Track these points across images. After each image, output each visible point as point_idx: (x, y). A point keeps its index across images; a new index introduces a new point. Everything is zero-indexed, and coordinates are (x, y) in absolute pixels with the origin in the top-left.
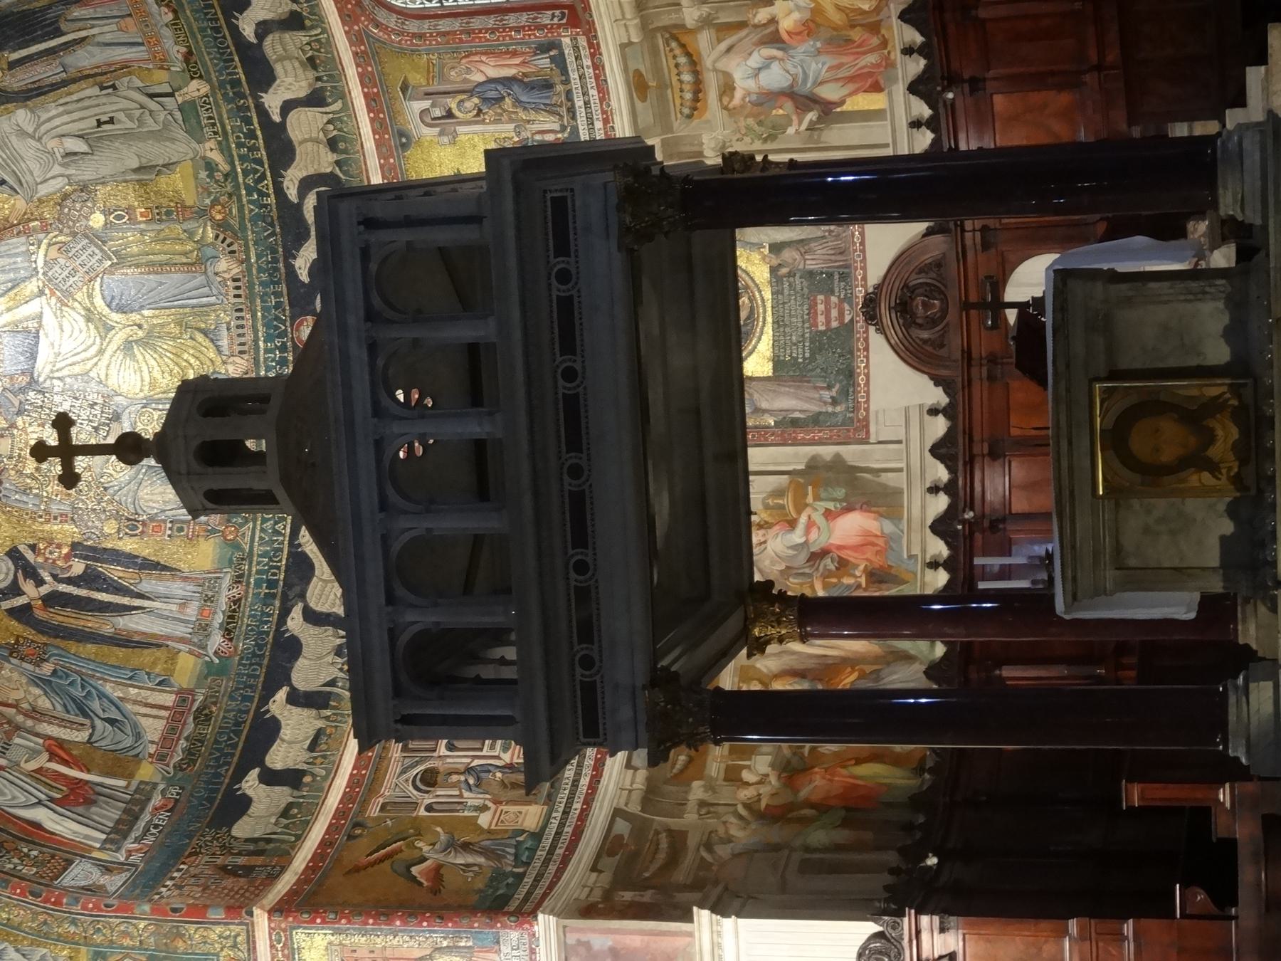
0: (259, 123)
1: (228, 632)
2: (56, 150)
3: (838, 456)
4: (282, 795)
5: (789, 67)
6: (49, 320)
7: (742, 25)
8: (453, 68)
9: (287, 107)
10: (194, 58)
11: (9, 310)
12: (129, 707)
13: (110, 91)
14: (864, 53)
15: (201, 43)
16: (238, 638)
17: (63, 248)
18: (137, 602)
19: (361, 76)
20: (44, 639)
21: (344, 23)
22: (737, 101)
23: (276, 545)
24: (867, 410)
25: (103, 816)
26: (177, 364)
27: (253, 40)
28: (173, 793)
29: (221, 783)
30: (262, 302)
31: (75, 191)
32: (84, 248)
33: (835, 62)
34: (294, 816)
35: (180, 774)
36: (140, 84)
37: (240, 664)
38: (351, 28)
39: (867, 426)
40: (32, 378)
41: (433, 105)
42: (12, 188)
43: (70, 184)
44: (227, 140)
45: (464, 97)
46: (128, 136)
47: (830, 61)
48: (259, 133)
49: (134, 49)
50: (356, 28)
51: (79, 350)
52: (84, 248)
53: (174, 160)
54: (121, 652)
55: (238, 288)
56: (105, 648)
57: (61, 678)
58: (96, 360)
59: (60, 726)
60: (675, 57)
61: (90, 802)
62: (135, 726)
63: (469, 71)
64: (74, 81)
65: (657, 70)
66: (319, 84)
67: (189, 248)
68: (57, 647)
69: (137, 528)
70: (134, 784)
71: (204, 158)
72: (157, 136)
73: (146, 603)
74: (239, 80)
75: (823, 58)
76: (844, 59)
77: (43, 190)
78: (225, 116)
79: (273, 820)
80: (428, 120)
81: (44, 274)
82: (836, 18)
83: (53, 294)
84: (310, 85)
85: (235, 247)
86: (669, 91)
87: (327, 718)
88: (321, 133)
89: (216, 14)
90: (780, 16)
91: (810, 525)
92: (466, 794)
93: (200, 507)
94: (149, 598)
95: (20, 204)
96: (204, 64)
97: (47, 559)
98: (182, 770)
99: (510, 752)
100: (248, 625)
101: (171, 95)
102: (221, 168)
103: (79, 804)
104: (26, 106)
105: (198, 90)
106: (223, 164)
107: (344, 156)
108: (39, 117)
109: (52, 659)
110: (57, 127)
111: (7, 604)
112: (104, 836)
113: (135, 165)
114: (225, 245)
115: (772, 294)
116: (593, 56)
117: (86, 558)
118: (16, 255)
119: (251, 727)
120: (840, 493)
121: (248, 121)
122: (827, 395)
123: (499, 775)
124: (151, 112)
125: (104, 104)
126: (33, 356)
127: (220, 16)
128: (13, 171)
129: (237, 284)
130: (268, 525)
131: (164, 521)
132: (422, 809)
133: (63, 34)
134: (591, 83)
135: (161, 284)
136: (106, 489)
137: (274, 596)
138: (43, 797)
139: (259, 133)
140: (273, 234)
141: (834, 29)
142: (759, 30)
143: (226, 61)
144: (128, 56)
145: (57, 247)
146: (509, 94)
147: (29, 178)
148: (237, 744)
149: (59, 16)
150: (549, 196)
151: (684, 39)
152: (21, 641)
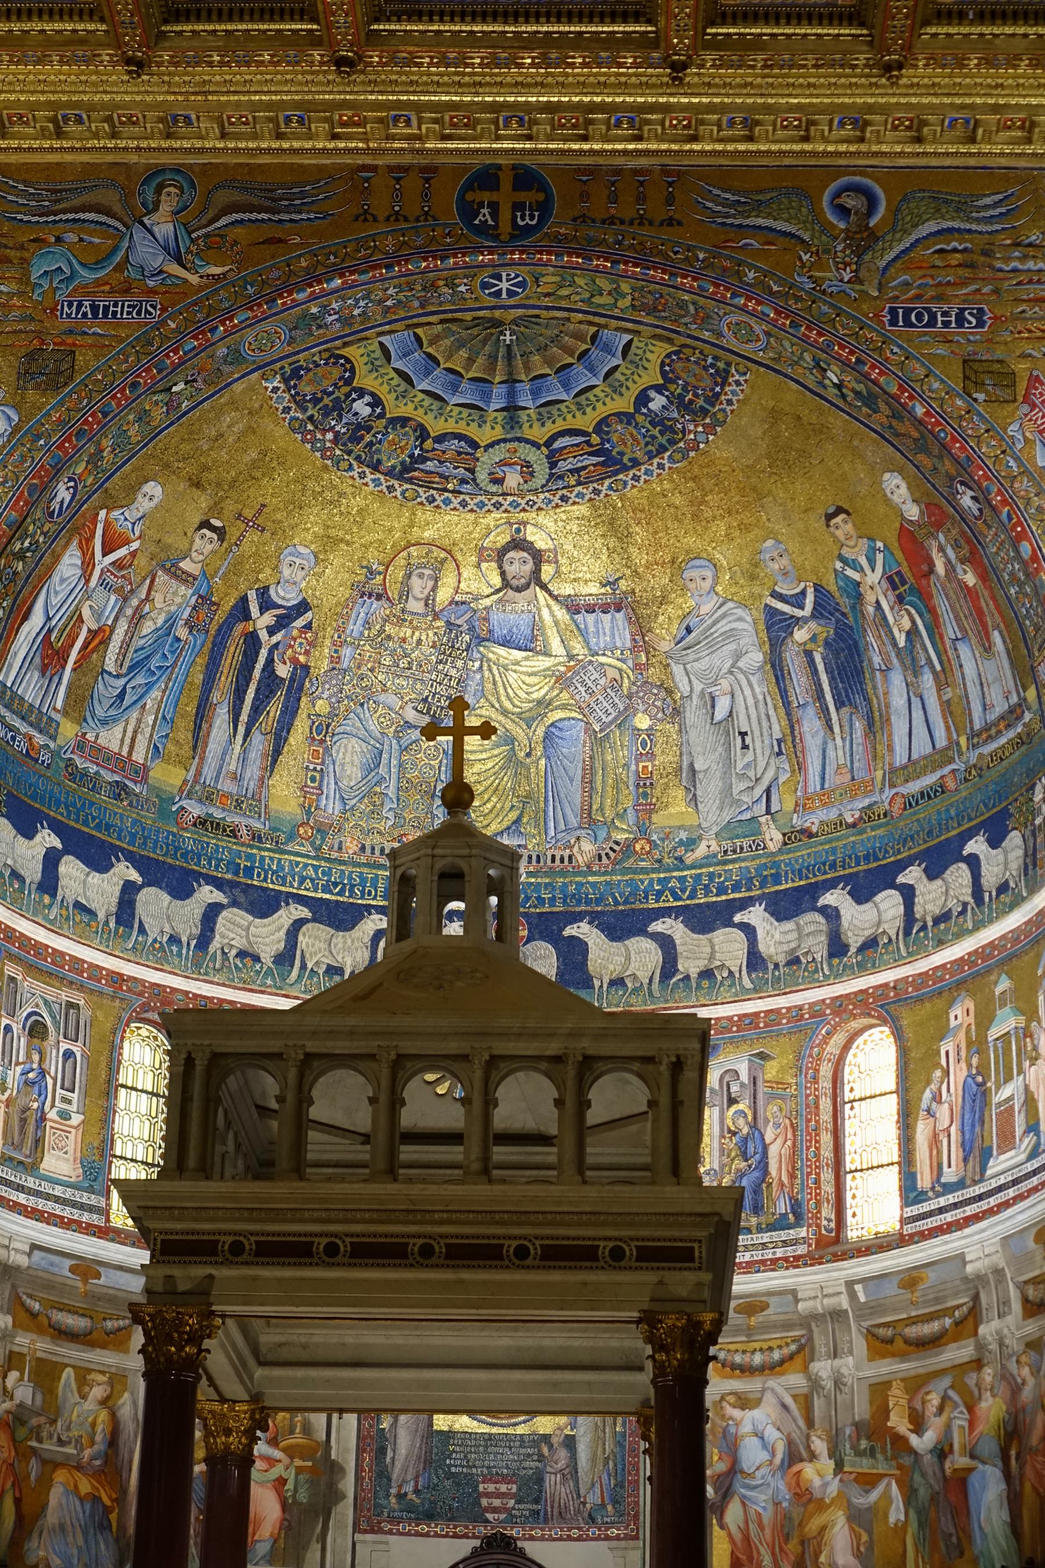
0: (734, 900)
1: (202, 822)
3: (343, 1497)
4: (33, 872)
5: (763, 1471)
6: (543, 663)
7: (810, 1423)
8: (781, 1110)
9: (749, 930)
11: (556, 623)
12: (135, 715)
13: (776, 749)
14: (773, 1554)
15: (820, 848)
16: (195, 833)
17: (615, 684)
18: (241, 729)
19: (777, 1011)
20: (213, 632)
21: (834, 999)
22: (730, 1411)
23: (289, 878)
24: (390, 1532)
25: (29, 683)
26: (487, 789)
27: (821, 902)
28: (45, 757)
29: (49, 808)
30: (546, 884)
31: (675, 702)
32: (614, 705)
33: (765, 1521)
34: (11, 885)
35: (62, 765)
36: (781, 781)
37: (169, 832)
38: (828, 1006)
39: (372, 1531)
40: (485, 640)
41: (742, 1085)
42: (682, 639)
43: (682, 698)
45: (750, 1118)
46: (729, 762)
47: (767, 1517)
48: (724, 898)
49: (818, 779)
50: (828, 1012)
51: (509, 690)
52: (614, 705)
53: (700, 807)
54: (191, 709)
55: (562, 860)
56: (198, 693)
57: (171, 645)
58: (497, 705)
59: (122, 642)
60: (780, 1347)
61: (43, 673)
62: (115, 720)
63: (777, 1126)
64: (788, 714)
65: (767, 1327)
66: (771, 966)
67: (609, 813)
68: (203, 645)
69: (318, 734)
70: (57, 716)
71: (700, 838)
72: (727, 790)
73: (239, 738)
74: (780, 884)
75: (770, 1508)
76: (768, 1532)
77: (677, 670)
78: (743, 865)
79: (9, 862)
80: (727, 1078)
81: (591, 662)
82: (813, 1525)
83: (569, 668)
84: (770, 957)
85: (605, 860)
86: (744, 1339)
87: (107, 922)
88: (719, 963)
89: (850, 867)
90: (818, 1465)
91: (271, 1462)
92: (19, 1069)
93: (398, 862)
94: (245, 740)
95: (665, 646)
97: (295, 639)
98: (67, 766)
99: (58, 1119)
100: (208, 844)
101: (768, 812)
103: (43, 659)
107: (694, 985)
109: (191, 638)
111: (252, 595)
112: (9, 684)
113: (697, 767)
114: (608, 850)
115: (521, 1435)
116: (786, 1259)
117: (292, 680)
118: (613, 636)
119: (104, 841)
120: (303, 1497)
121: (736, 888)
122: (409, 1488)
123: (35, 1105)
124: (752, 788)
126: (506, 643)
127: (847, 872)
129: (566, 860)
130: (311, 872)
131: (323, 763)
132: (8, 1022)
133: (837, 710)
134: (758, 1255)
135: (572, 781)
136: (362, 705)
137: (237, 874)
138: (54, 622)
139: (724, 898)
140: (617, 903)
141: (800, 1524)
142: (804, 1440)
144: (811, 771)
145: (618, 677)
146: (750, 1166)
147: (691, 657)
148: (88, 826)
149: (856, 708)
150: (696, 1245)
151: (798, 1360)
152: (214, 608)
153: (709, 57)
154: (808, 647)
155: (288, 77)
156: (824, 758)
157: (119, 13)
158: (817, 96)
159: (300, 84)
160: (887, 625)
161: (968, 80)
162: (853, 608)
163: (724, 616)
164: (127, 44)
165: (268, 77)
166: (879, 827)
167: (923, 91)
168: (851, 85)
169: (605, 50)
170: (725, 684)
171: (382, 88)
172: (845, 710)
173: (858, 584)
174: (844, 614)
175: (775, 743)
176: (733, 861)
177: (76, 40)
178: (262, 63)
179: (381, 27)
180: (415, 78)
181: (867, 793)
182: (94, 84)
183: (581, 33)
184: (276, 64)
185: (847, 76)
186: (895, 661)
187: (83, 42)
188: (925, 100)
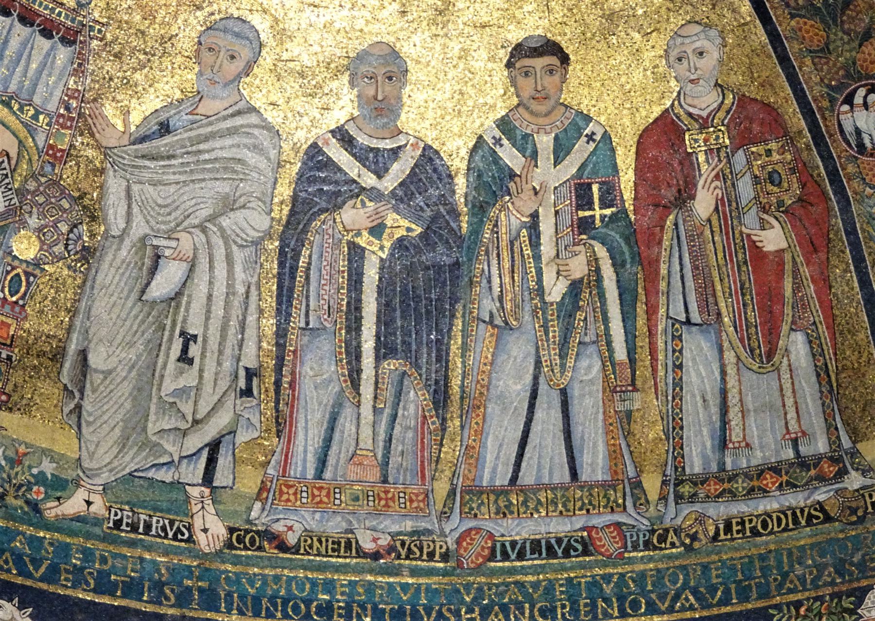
2: (173, 244)
10: (270, 550)
13: (242, 383)
44: (105, 538)
48: (106, 600)
49: (311, 460)
71: (78, 486)
77: (115, 185)
96: (248, 562)
102: (49, 505)
104: (268, 235)
105: (205, 530)
106: (59, 511)
108: (242, 246)
110: (211, 268)
113: (94, 360)
124: (185, 433)
125: (219, 364)
128: (173, 157)
139: (106, 600)
143: (257, 600)
145: (13, 154)
147: (146, 175)
149: (418, 367)
154: (362, 242)
156: (331, 429)
160: (537, 257)
162: (480, 209)
163: (232, 132)
166: (430, 572)
170: (186, 242)
172: (391, 365)
173: (512, 175)
174: (455, 213)
175: (242, 373)
176: (132, 544)
181: (419, 513)
186: (527, 317)
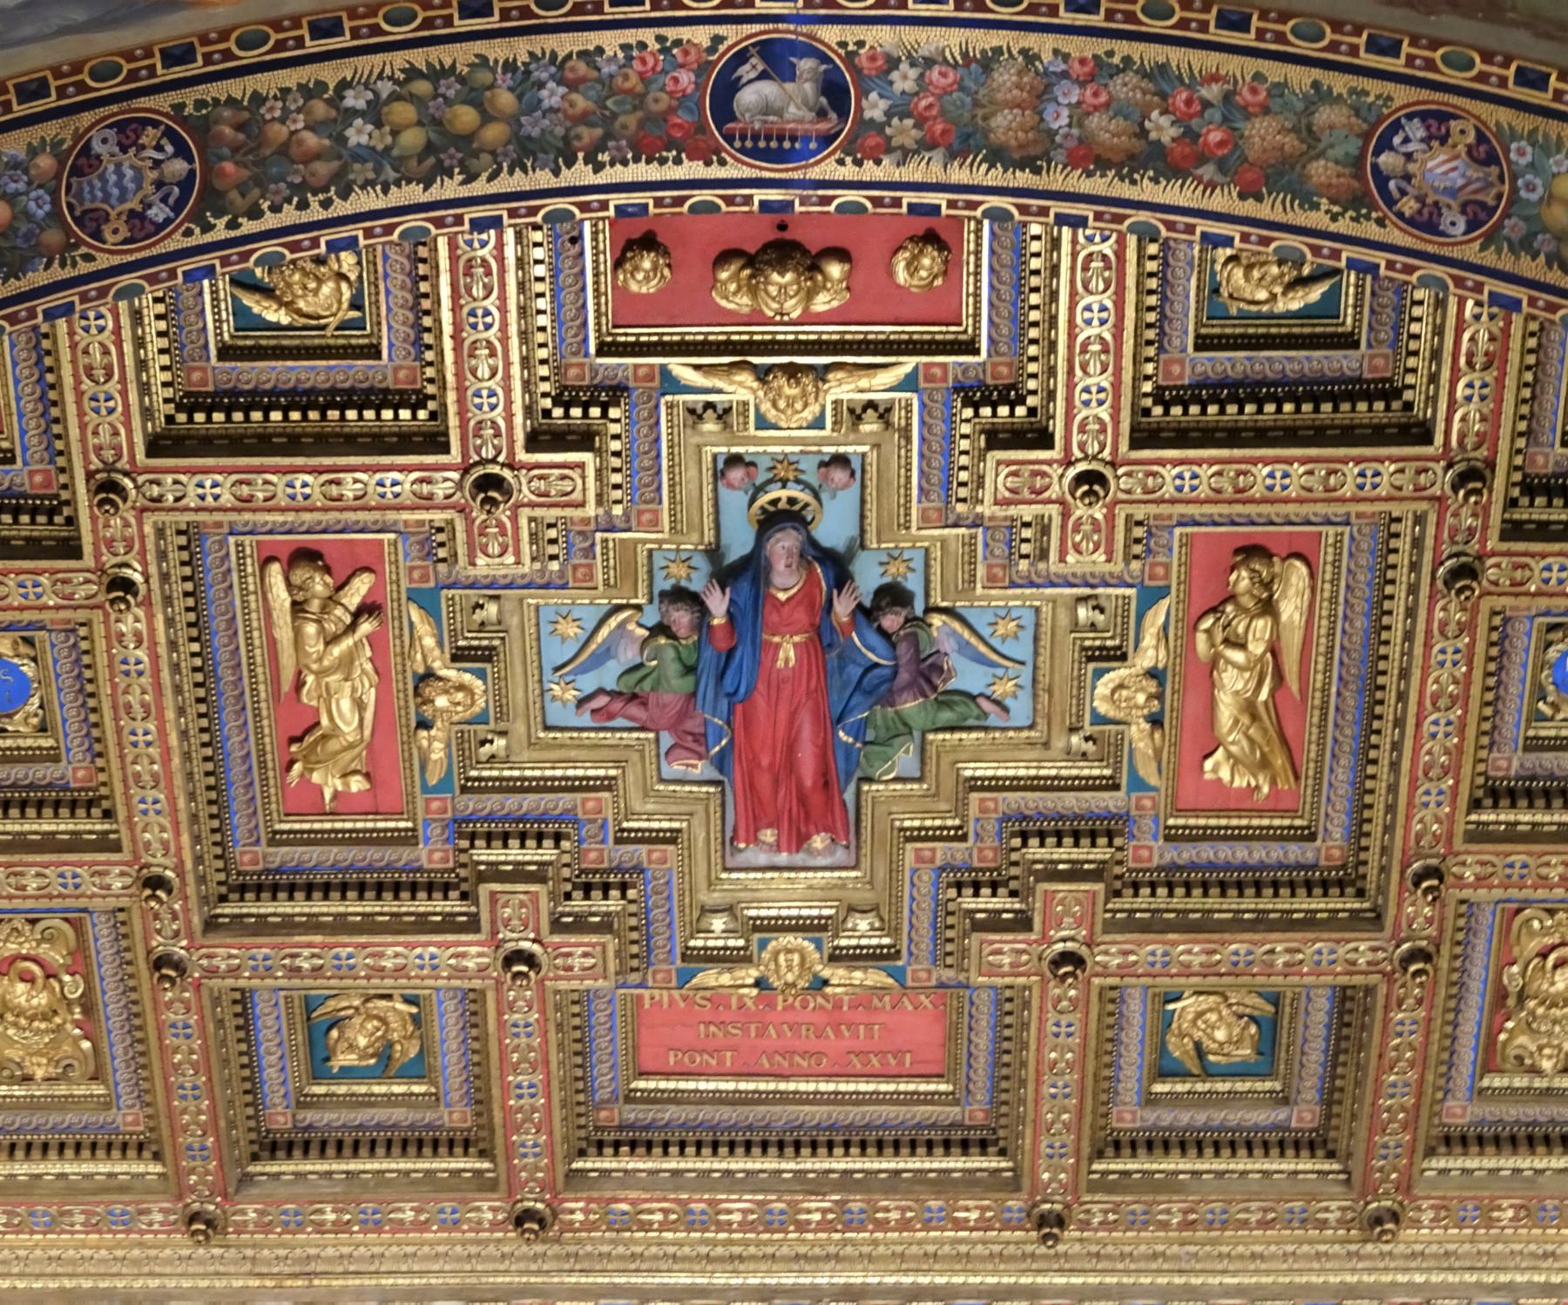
153: (1097, 1207)
155: (441, 1249)
157: (185, 1129)
158: (1268, 1272)
159: (459, 1259)
161: (1500, 1247)
164: (192, 1189)
165: (410, 1249)
167: (1432, 1263)
168: (1318, 1256)
169: (938, 1194)
171: (586, 1265)
177: (112, 1186)
178: (400, 1226)
179: (589, 1165)
180: (639, 1249)
182: (136, 1262)
183: (897, 1172)
184: (423, 1227)
185: (1311, 1242)
187: (123, 1189)
188: (1436, 1278)
